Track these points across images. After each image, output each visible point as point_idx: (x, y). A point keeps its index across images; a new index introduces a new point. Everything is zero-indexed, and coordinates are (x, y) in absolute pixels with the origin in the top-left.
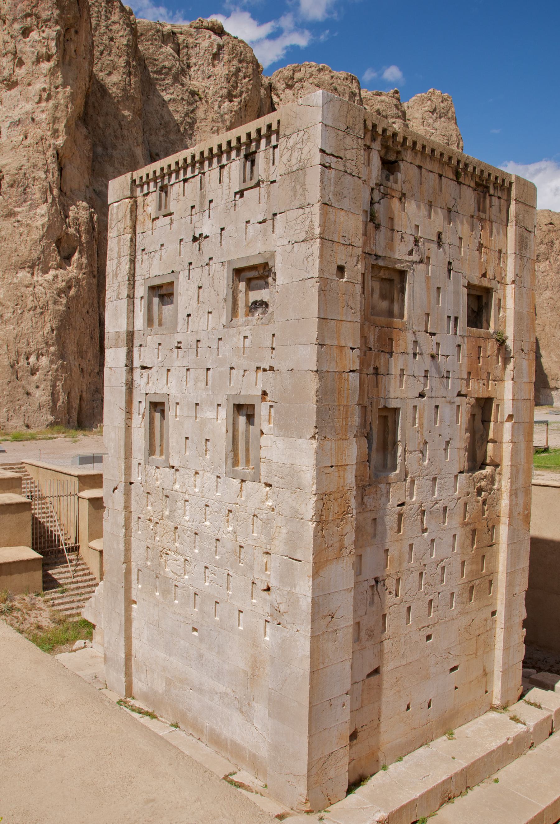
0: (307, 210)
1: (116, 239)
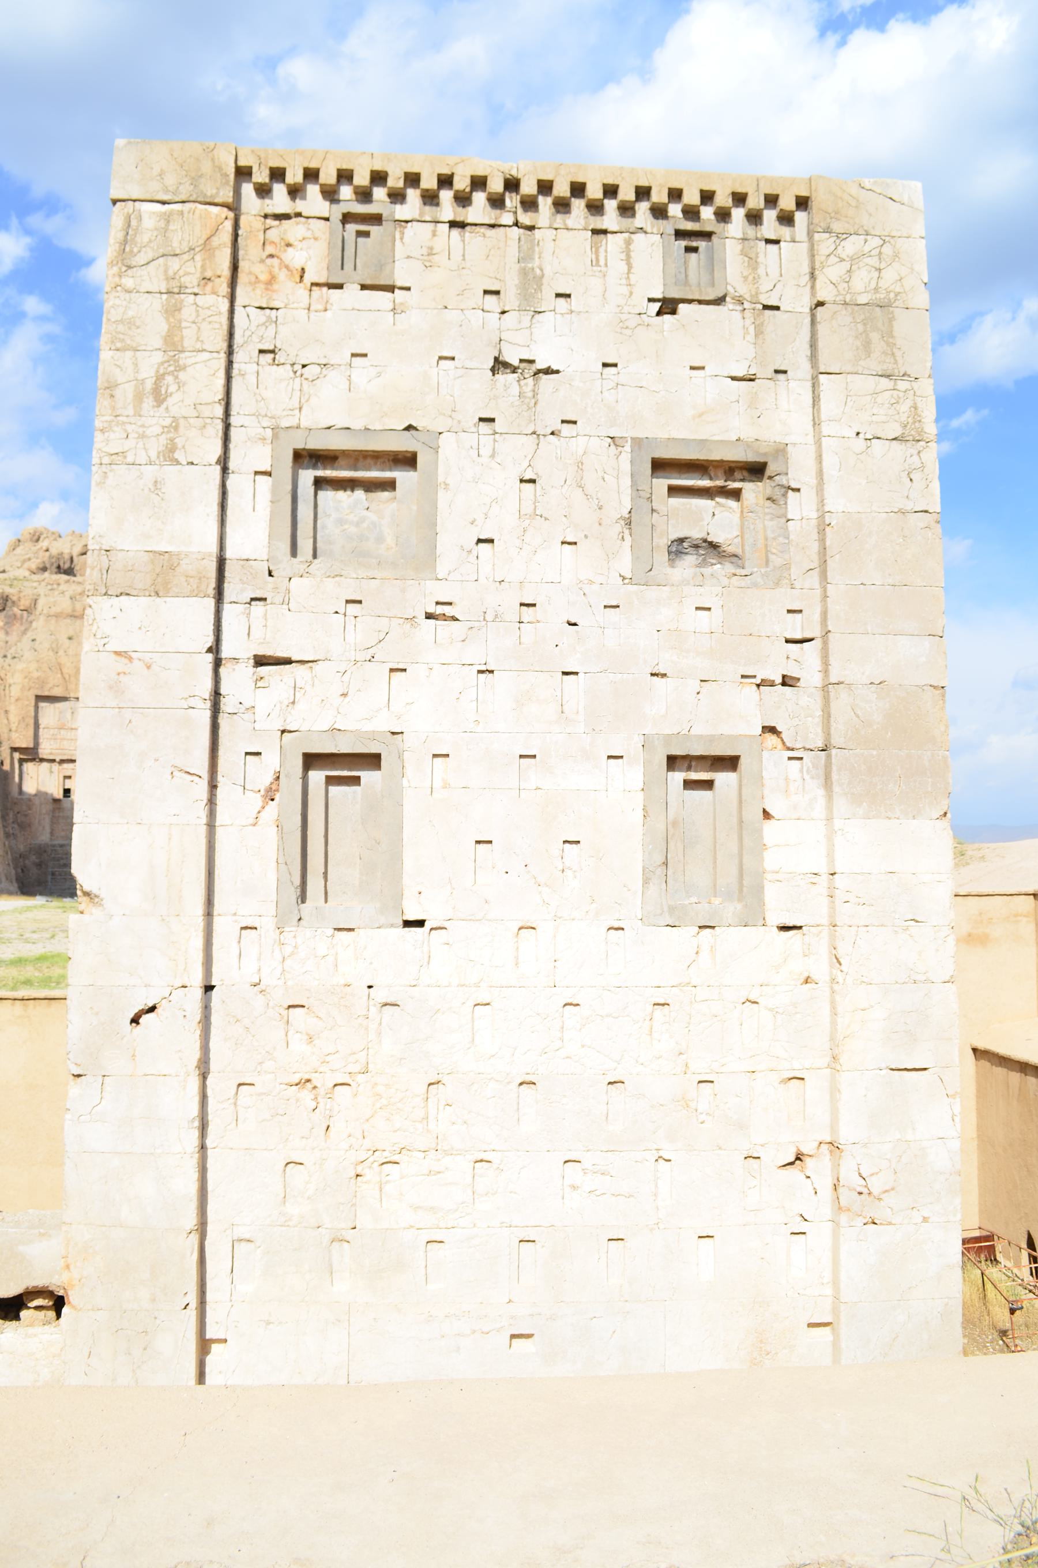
0: (902, 385)
1: (158, 302)
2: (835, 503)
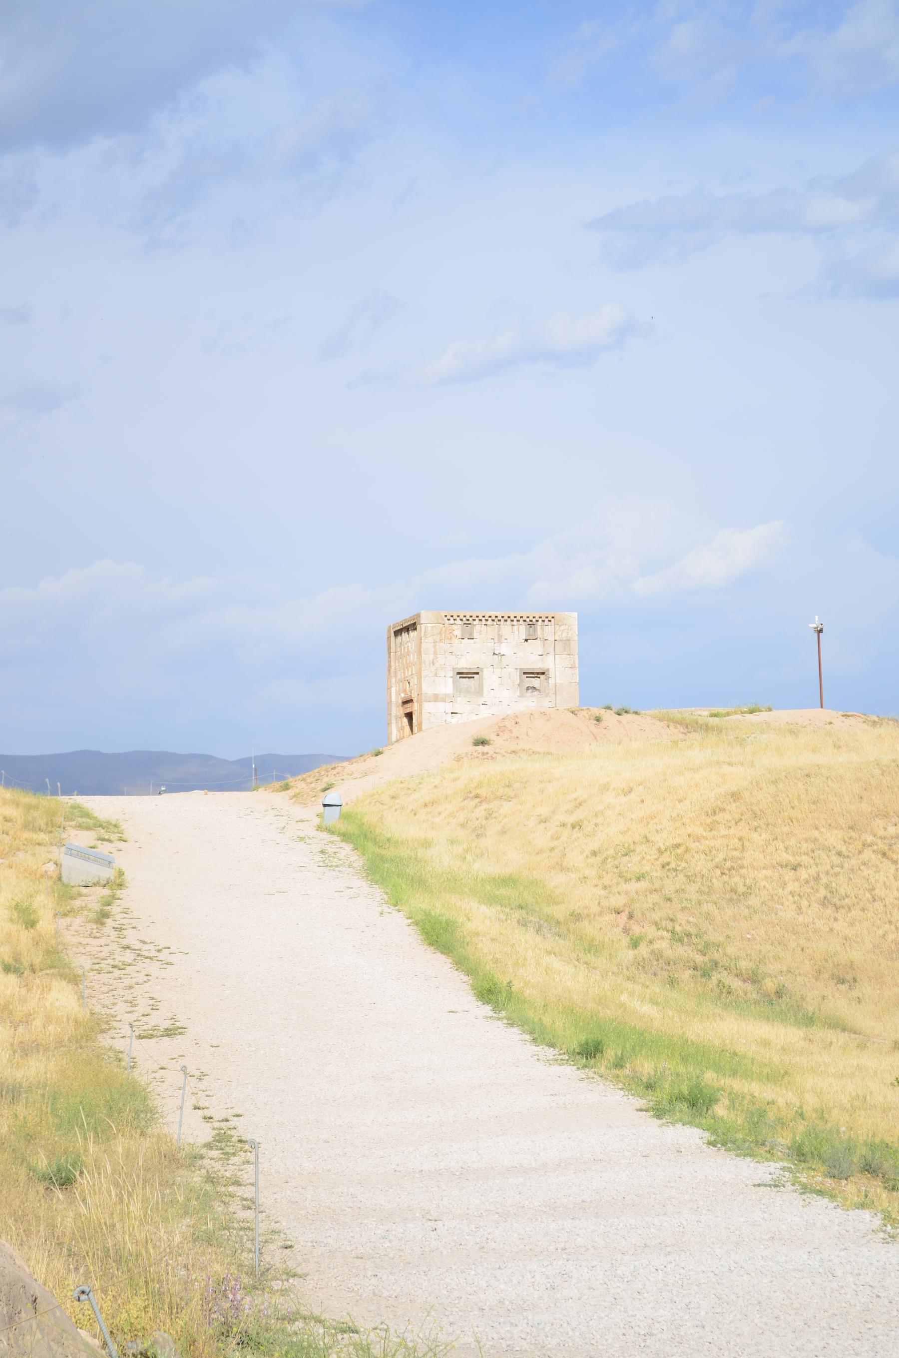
2: (558, 681)
